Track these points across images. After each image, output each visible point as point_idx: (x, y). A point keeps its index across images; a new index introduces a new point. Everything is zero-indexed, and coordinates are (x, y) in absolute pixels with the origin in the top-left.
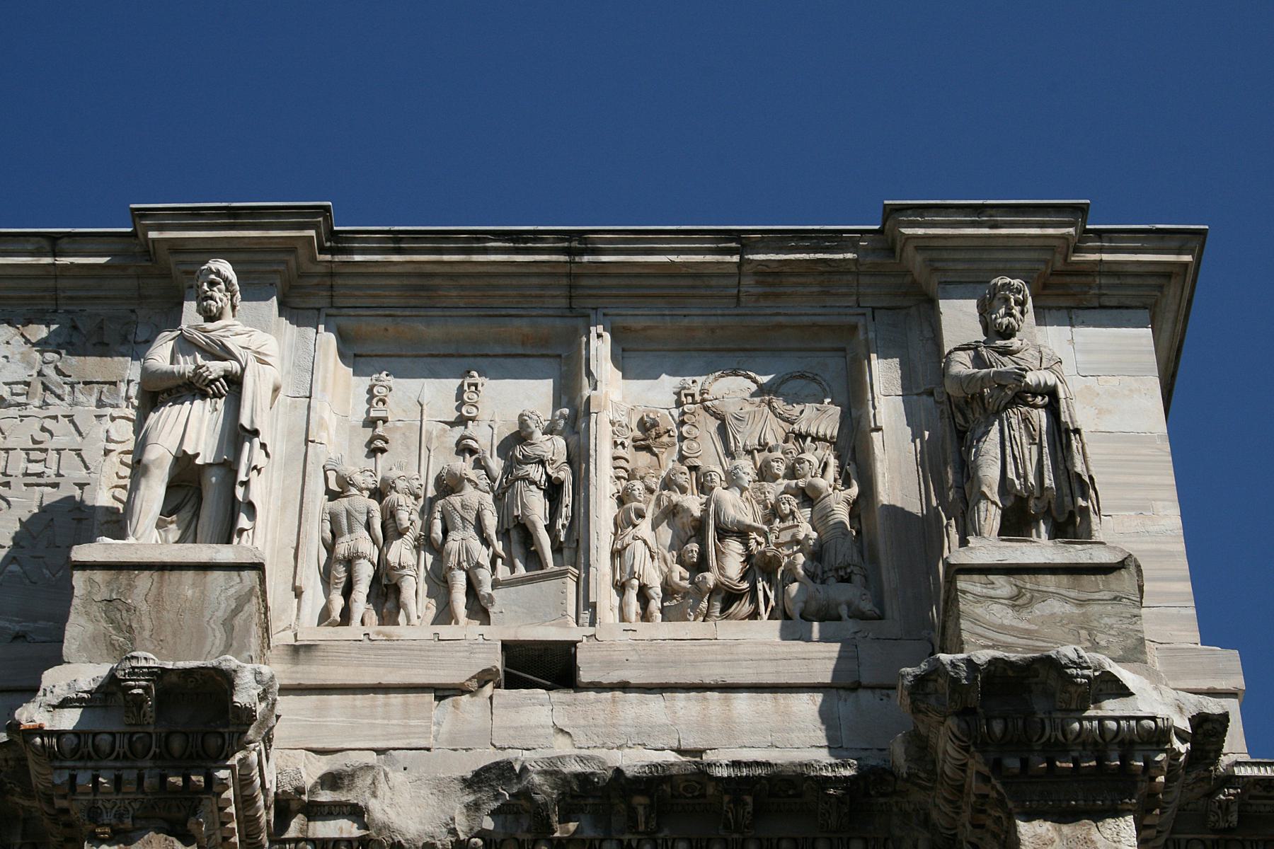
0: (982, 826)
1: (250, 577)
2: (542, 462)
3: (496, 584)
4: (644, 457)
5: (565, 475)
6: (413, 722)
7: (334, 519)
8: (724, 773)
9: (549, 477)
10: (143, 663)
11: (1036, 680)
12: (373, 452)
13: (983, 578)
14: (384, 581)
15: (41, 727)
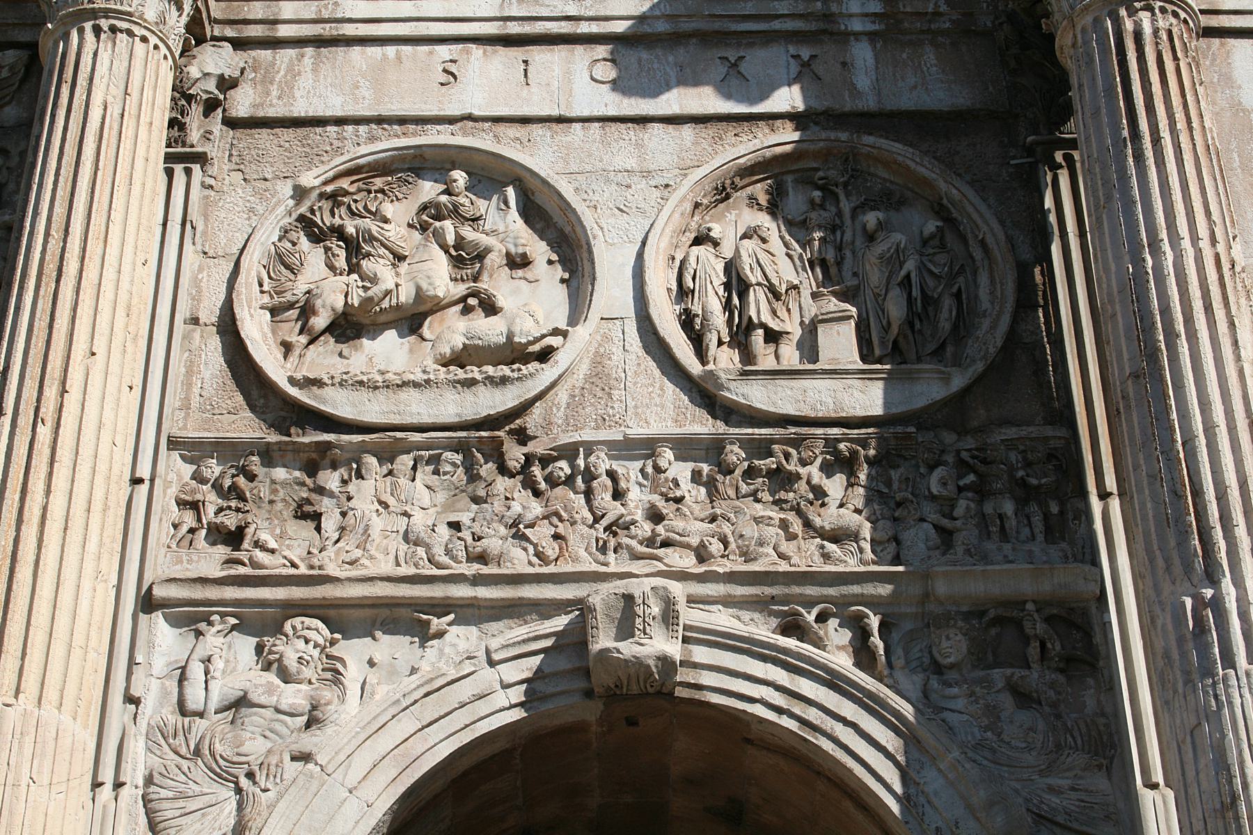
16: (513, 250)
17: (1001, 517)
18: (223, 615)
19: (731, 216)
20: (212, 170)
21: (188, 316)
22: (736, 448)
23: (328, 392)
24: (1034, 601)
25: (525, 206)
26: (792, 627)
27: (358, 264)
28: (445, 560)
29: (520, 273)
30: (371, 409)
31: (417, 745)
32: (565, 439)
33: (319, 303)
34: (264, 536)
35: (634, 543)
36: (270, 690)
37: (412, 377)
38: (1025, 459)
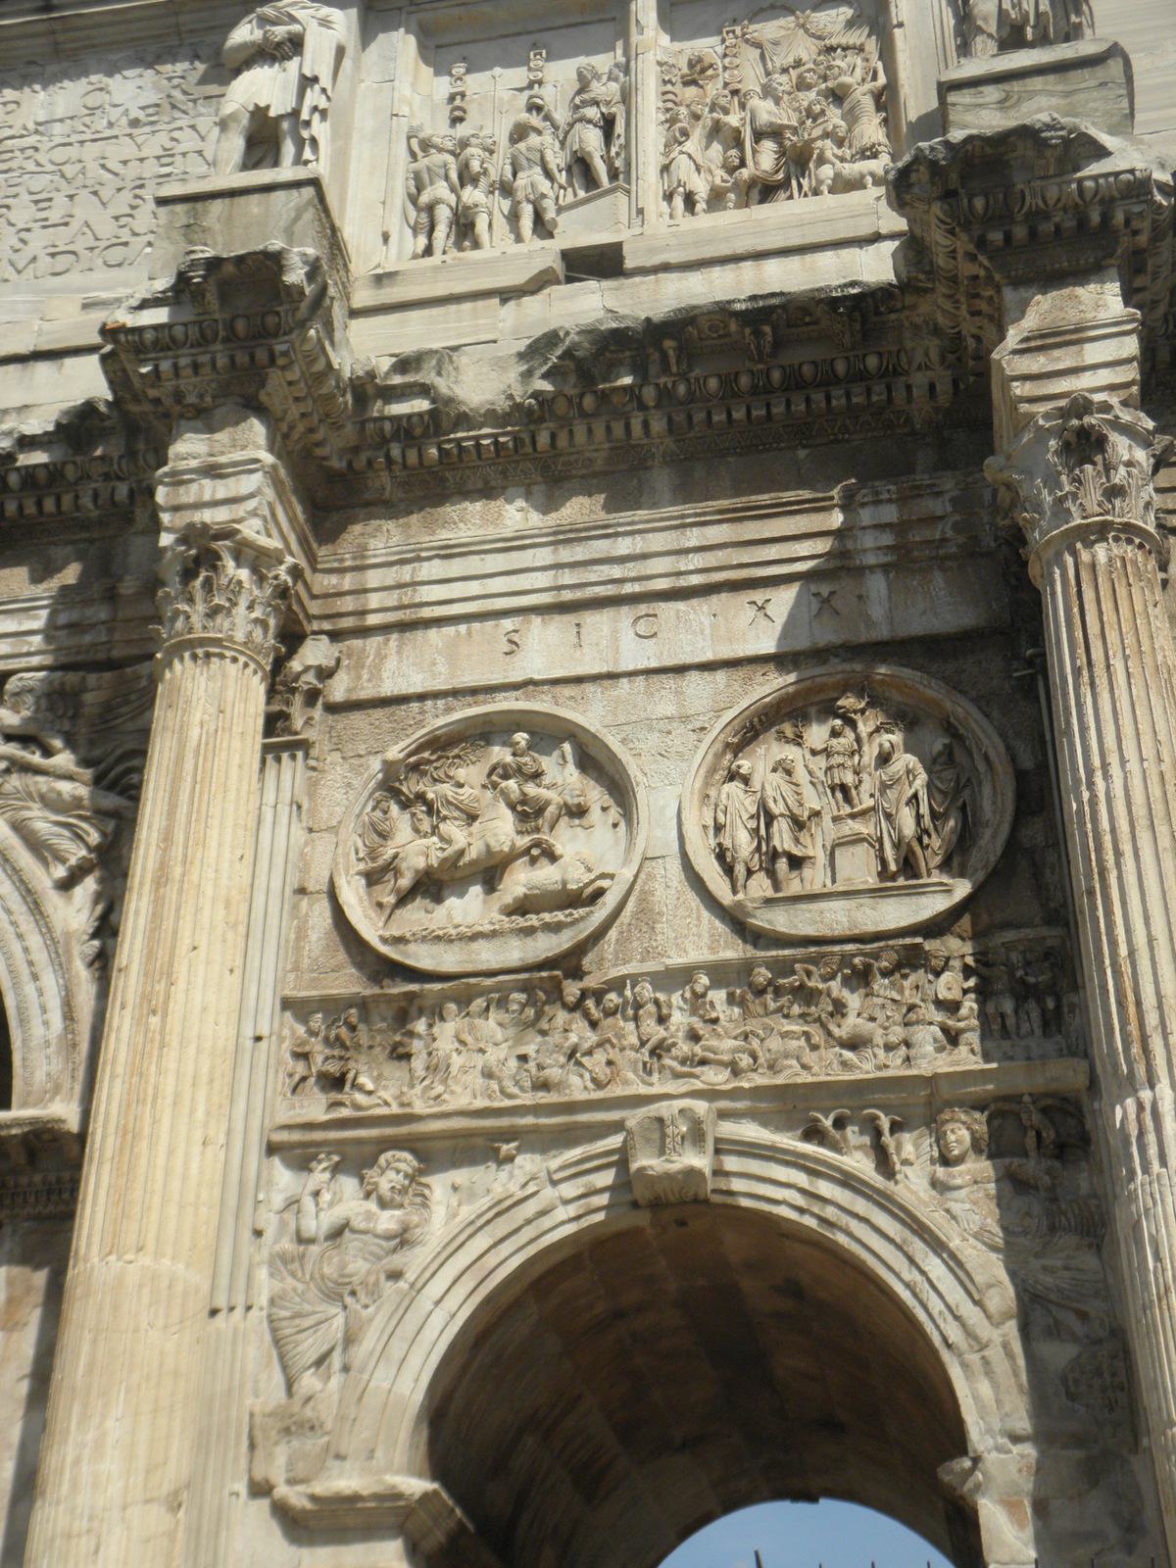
0: (978, 313)
1: (308, 192)
2: (596, 103)
3: (560, 210)
4: (692, 91)
5: (619, 111)
6: (481, 322)
7: (417, 177)
8: (744, 306)
9: (602, 114)
10: (201, 255)
11: (1015, 154)
12: (456, 121)
13: (973, 91)
14: (462, 221)
15: (124, 326)
16: (570, 801)
17: (1002, 1016)
18: (329, 1154)
19: (761, 750)
20: (314, 752)
21: (296, 886)
22: (763, 970)
23: (412, 947)
24: (1030, 1094)
25: (581, 759)
26: (813, 1134)
27: (437, 827)
28: (516, 1090)
29: (577, 822)
30: (447, 959)
31: (492, 1260)
32: (615, 973)
33: (404, 866)
34: (363, 1080)
35: (674, 1064)
36: (369, 1216)
37: (480, 929)
38: (1024, 958)
